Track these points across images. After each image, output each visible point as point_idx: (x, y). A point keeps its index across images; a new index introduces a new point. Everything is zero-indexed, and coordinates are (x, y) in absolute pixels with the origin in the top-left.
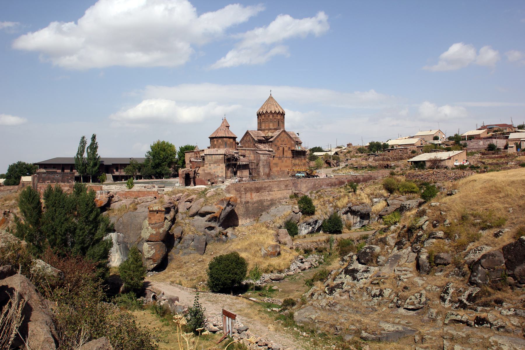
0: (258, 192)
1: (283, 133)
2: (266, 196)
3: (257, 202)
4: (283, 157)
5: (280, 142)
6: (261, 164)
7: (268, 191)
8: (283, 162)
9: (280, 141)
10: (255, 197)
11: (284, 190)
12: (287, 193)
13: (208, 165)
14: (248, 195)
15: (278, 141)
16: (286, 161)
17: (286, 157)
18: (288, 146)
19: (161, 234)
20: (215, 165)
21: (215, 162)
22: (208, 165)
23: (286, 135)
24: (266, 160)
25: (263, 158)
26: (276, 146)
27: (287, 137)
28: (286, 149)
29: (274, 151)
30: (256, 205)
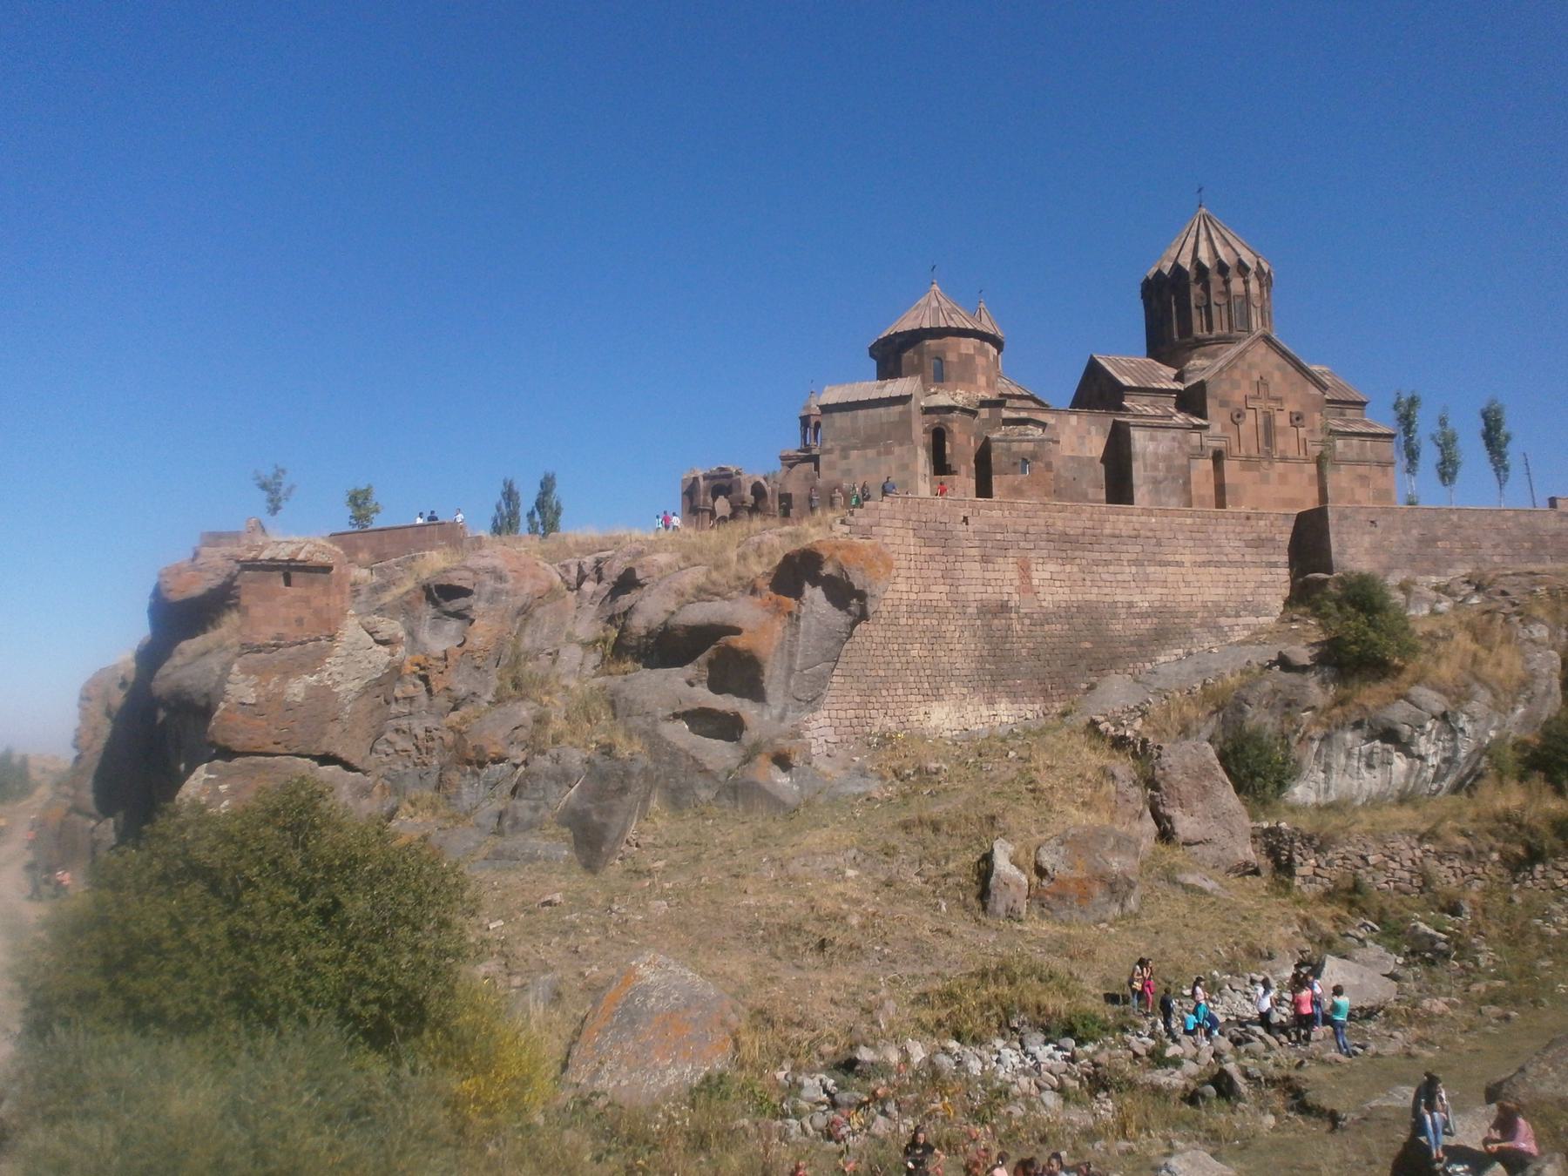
0: (1066, 560)
1: (1262, 348)
2: (1129, 591)
3: (1067, 613)
4: (1269, 456)
5: (1246, 389)
6: (1139, 473)
7: (1137, 562)
8: (1265, 480)
9: (1245, 384)
10: (1053, 585)
11: (1241, 564)
12: (1262, 584)
13: (835, 456)
14: (1007, 570)
15: (1236, 385)
16: (1283, 478)
17: (1284, 459)
18: (1288, 407)
19: (290, 708)
20: (871, 453)
21: (869, 441)
22: (835, 456)
23: (1274, 358)
24: (1168, 458)
25: (1151, 447)
26: (1224, 404)
27: (1278, 367)
28: (1282, 420)
29: (1216, 428)
30: (1056, 628)
